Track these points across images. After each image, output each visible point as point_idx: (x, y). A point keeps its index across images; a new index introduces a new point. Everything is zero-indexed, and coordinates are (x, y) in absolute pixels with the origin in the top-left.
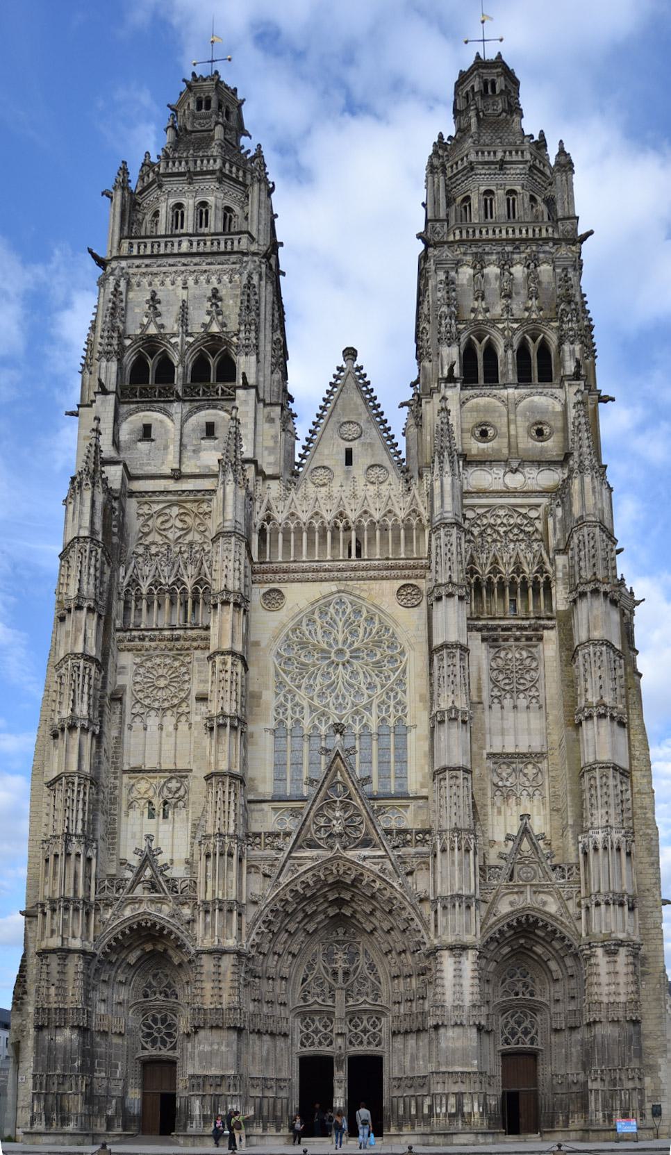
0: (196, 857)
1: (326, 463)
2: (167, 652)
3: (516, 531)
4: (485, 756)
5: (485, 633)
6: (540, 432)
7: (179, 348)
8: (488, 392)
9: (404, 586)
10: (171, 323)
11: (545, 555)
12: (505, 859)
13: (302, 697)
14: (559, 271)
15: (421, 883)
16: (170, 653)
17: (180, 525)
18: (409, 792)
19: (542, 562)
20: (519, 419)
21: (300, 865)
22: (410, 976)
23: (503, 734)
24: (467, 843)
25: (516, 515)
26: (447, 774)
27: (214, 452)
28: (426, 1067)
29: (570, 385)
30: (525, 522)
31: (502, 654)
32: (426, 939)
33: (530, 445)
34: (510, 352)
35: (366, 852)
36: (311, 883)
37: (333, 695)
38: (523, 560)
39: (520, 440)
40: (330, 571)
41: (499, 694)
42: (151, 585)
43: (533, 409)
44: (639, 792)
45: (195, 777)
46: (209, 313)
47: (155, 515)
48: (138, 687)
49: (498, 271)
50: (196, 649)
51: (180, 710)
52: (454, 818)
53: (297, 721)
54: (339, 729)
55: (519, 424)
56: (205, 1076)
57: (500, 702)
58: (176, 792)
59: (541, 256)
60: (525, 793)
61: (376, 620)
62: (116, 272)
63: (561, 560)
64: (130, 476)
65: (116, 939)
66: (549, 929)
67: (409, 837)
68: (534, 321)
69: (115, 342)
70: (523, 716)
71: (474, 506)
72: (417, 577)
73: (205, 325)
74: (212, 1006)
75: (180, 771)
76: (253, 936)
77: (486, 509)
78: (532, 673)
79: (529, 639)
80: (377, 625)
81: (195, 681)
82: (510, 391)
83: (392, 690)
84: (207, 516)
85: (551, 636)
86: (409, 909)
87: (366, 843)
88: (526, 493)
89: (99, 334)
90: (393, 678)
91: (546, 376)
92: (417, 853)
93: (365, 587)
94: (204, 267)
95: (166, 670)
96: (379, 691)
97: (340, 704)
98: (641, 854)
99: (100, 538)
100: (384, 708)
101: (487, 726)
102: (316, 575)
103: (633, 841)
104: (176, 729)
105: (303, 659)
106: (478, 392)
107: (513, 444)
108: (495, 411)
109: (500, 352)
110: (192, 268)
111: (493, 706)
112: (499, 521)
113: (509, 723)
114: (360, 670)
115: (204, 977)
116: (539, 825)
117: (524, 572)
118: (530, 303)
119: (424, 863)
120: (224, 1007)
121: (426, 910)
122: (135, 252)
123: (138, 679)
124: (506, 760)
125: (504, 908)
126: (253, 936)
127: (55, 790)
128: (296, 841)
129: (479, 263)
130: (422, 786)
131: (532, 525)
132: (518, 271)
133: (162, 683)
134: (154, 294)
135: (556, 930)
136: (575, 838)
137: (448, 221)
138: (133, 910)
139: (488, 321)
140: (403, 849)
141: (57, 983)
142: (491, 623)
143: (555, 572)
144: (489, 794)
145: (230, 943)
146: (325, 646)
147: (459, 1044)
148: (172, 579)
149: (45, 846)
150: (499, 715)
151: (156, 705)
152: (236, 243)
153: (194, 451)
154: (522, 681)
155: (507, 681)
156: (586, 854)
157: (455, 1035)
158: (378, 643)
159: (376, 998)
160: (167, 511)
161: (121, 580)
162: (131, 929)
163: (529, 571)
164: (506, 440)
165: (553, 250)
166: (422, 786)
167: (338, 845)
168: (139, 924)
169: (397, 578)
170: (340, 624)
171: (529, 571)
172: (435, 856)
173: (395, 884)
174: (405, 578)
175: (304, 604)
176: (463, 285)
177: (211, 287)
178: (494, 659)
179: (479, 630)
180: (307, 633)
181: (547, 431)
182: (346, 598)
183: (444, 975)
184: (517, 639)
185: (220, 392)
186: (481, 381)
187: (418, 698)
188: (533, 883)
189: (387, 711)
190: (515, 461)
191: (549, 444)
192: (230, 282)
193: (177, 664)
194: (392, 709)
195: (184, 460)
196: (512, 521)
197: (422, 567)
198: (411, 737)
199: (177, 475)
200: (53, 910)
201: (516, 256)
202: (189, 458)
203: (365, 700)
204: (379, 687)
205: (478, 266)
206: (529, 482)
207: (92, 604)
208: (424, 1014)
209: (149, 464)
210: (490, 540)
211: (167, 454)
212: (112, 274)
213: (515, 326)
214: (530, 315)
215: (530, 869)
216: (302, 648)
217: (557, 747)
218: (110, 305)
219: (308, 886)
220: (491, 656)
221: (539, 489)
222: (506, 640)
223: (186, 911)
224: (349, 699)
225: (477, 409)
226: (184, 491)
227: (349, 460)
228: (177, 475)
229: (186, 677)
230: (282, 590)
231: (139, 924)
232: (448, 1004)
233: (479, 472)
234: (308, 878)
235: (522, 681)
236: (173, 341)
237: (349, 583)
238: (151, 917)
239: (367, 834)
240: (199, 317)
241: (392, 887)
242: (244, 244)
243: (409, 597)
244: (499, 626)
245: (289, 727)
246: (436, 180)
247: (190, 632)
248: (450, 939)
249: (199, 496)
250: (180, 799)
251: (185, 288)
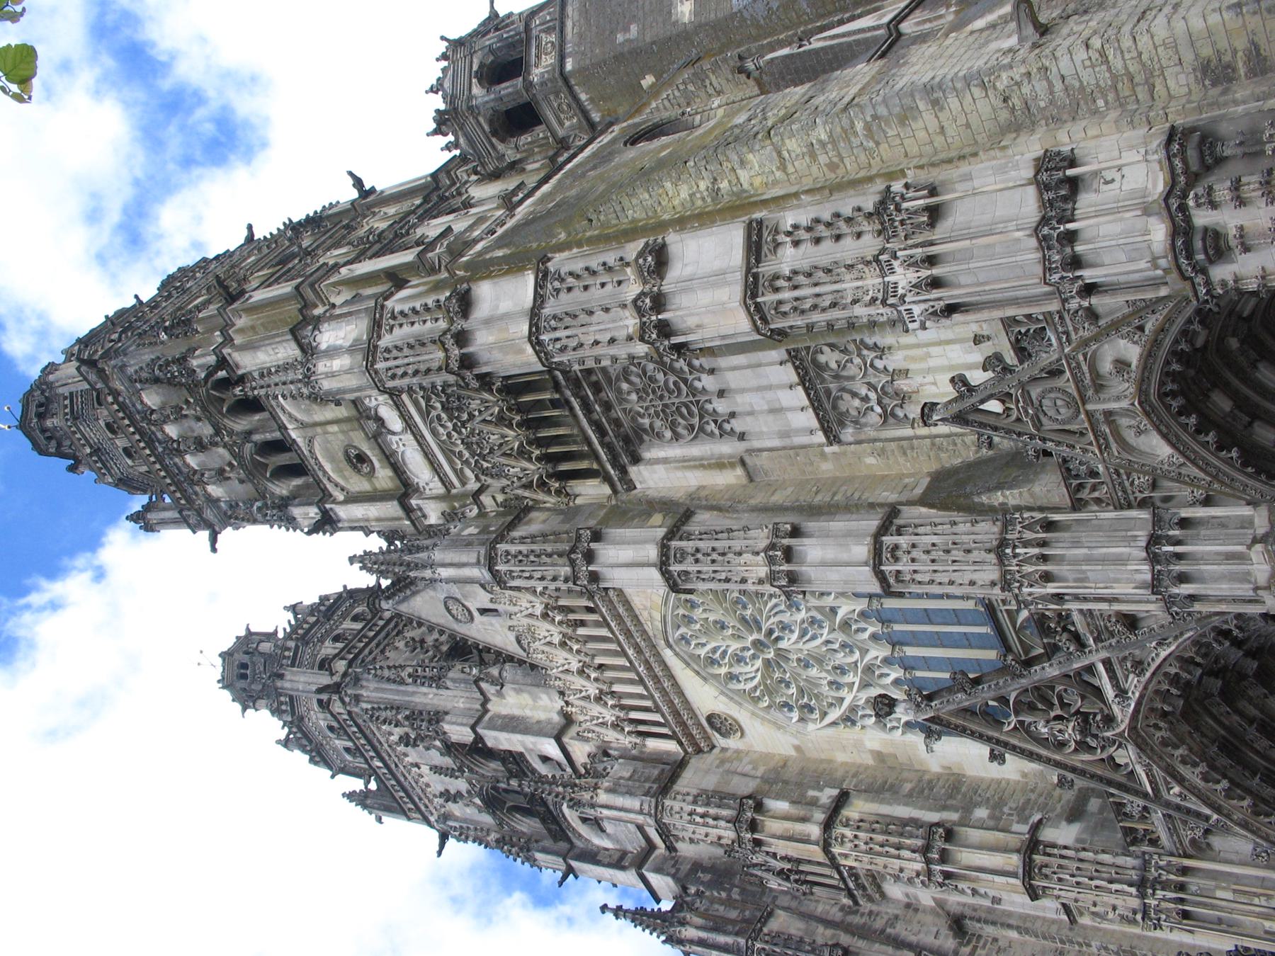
4: (835, 448)
5: (625, 459)
8: (312, 462)
24: (1029, 527)
29: (238, 366)
40: (647, 663)
71: (455, 471)
79: (597, 388)
98: (921, 135)
101: (776, 443)
111: (738, 429)
124: (828, 406)
125: (1160, 450)
132: (172, 430)
139: (241, 465)
146: (759, 663)
150: (749, 419)
154: (672, 386)
155: (684, 410)
178: (659, 436)
179: (623, 471)
184: (607, 406)
201: (159, 435)
215: (1046, 402)
222: (617, 423)
225: (339, 471)
233: (410, 467)
237: (651, 634)
240: (437, 758)
244: (602, 444)
251: (417, 766)
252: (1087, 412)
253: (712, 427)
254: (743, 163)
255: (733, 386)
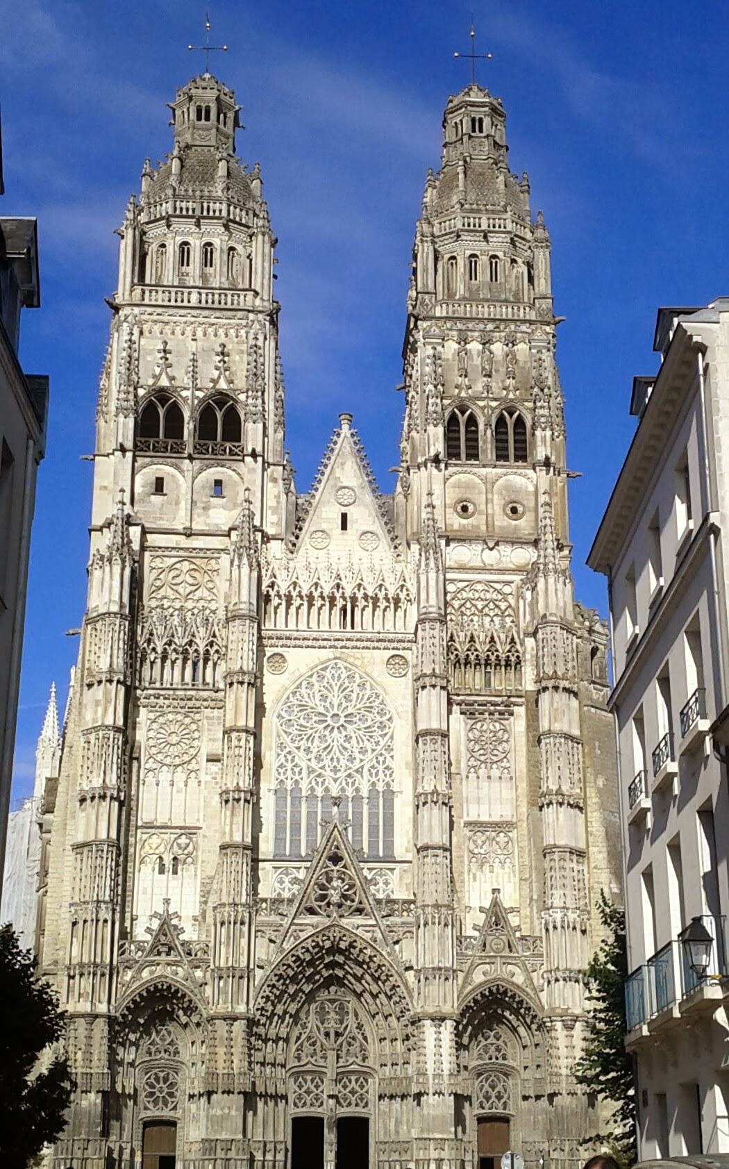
0: (210, 920)
1: (324, 527)
2: (179, 710)
3: (491, 606)
4: (462, 825)
6: (514, 510)
7: (189, 402)
9: (393, 656)
10: (184, 379)
11: (516, 636)
12: (479, 930)
13: (301, 759)
14: (534, 351)
15: (407, 952)
16: (183, 711)
17: (190, 581)
18: (396, 855)
19: (513, 641)
20: (496, 497)
21: (301, 931)
22: (396, 1039)
23: (479, 803)
25: (492, 590)
26: (430, 851)
27: (221, 510)
28: (409, 1131)
30: (500, 597)
31: (479, 724)
32: (410, 1007)
33: (505, 524)
34: (489, 432)
35: (359, 920)
36: (311, 949)
37: (329, 757)
38: (496, 639)
39: (496, 518)
41: (475, 764)
42: (166, 644)
43: (509, 488)
44: (596, 867)
45: (204, 836)
46: (217, 368)
47: (167, 570)
48: (151, 743)
49: (481, 347)
50: (206, 708)
51: (190, 767)
52: (435, 894)
53: (297, 782)
54: (337, 801)
55: (495, 501)
56: (217, 1140)
57: (476, 772)
58: (186, 848)
59: (519, 335)
60: (497, 860)
61: (368, 686)
62: (129, 319)
63: (530, 642)
64: (144, 532)
65: (134, 1001)
66: (517, 999)
67: (396, 906)
68: (511, 400)
69: (131, 397)
70: (495, 785)
72: (404, 649)
73: (212, 380)
74: (226, 1071)
75: (189, 828)
76: (259, 1000)
77: (466, 584)
78: (504, 744)
79: (501, 713)
80: (368, 692)
81: (205, 739)
82: (488, 470)
83: (381, 755)
84: (215, 573)
85: (520, 711)
86: (396, 976)
87: (360, 911)
88: (502, 571)
89: (113, 381)
90: (382, 743)
91: (522, 456)
92: (403, 923)
93: (358, 655)
94: (213, 320)
95: (177, 726)
96: (370, 755)
97: (335, 767)
99: (127, 611)
100: (374, 771)
101: (464, 794)
102: (316, 642)
103: (588, 919)
104: (186, 786)
105: (302, 721)
106: (460, 469)
107: (490, 523)
108: (474, 488)
109: (481, 427)
110: (201, 320)
112: (477, 595)
113: (484, 792)
114: (353, 735)
115: (217, 1043)
116: (509, 899)
117: (497, 651)
118: (508, 381)
119: (409, 932)
120: (236, 1071)
121: (410, 975)
122: (147, 302)
123: (152, 734)
124: (481, 829)
125: (478, 978)
126: (259, 1000)
127: (82, 853)
128: (298, 908)
129: (463, 340)
130: (407, 851)
131: (506, 601)
132: (498, 348)
133: (174, 739)
134: (166, 343)
135: (522, 1001)
136: (539, 911)
137: (435, 294)
138: (152, 973)
139: (470, 398)
140: (391, 918)
141: (83, 1047)
142: (468, 698)
143: (524, 653)
144: (466, 862)
145: (241, 1008)
146: (322, 710)
147: (438, 1112)
148: (186, 640)
149: (72, 909)
151: (168, 761)
152: (242, 297)
153: (204, 508)
154: (495, 752)
155: (482, 752)
156: (547, 930)
157: (435, 1103)
158: (369, 709)
159: (364, 1059)
160: (178, 566)
161: (139, 639)
162: (148, 991)
163: (502, 649)
164: (484, 517)
165: (529, 331)
166: (407, 851)
167: (335, 914)
168: (156, 987)
169: (388, 649)
170: (336, 688)
171: (502, 649)
172: (419, 927)
173: (384, 953)
174: (393, 649)
175: (304, 669)
176: (448, 360)
177: (220, 342)
178: (471, 729)
180: (306, 696)
181: (520, 509)
182: (341, 664)
183: (426, 1044)
184: (491, 714)
185: (228, 451)
186: (463, 455)
187: (404, 766)
188: (503, 954)
189: (377, 774)
190: (493, 540)
191: (522, 523)
192: (237, 337)
193: (187, 721)
194: (380, 773)
195: (195, 516)
196: (488, 596)
197: (408, 641)
198: (397, 801)
199: (189, 533)
200: (81, 975)
201: (496, 334)
202: (199, 516)
203: (357, 764)
204: (370, 751)
205: (462, 343)
206: (504, 559)
207: (122, 679)
208: (409, 1079)
209: (161, 519)
210: (468, 613)
211: (178, 509)
212: (125, 320)
213: (494, 404)
214: (508, 394)
215: (500, 941)
216: (301, 711)
217: (525, 818)
218: (124, 354)
219: (308, 950)
220: (469, 727)
221: (513, 567)
223: (198, 973)
224: (343, 762)
225: (458, 486)
226: (194, 549)
227: (344, 527)
228: (189, 533)
229: (196, 735)
230: (284, 654)
231: (156, 987)
232: (430, 1072)
234: (309, 944)
235: (495, 752)
236: (184, 394)
237: (344, 650)
238: (167, 980)
239: (361, 903)
240: (209, 370)
241: (382, 955)
242: (249, 300)
243: (397, 666)
244: (476, 702)
245: (289, 788)
246: (426, 248)
247: (201, 693)
248: (431, 1010)
249: (209, 554)
250: (189, 855)
252: (495, 957)
253: (472, 762)
254: (600, 852)
255: (492, 784)
